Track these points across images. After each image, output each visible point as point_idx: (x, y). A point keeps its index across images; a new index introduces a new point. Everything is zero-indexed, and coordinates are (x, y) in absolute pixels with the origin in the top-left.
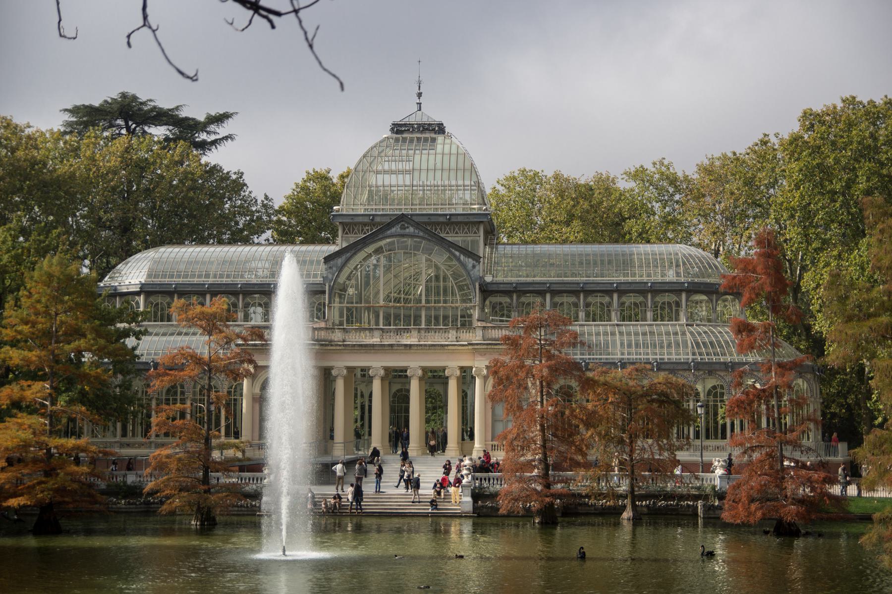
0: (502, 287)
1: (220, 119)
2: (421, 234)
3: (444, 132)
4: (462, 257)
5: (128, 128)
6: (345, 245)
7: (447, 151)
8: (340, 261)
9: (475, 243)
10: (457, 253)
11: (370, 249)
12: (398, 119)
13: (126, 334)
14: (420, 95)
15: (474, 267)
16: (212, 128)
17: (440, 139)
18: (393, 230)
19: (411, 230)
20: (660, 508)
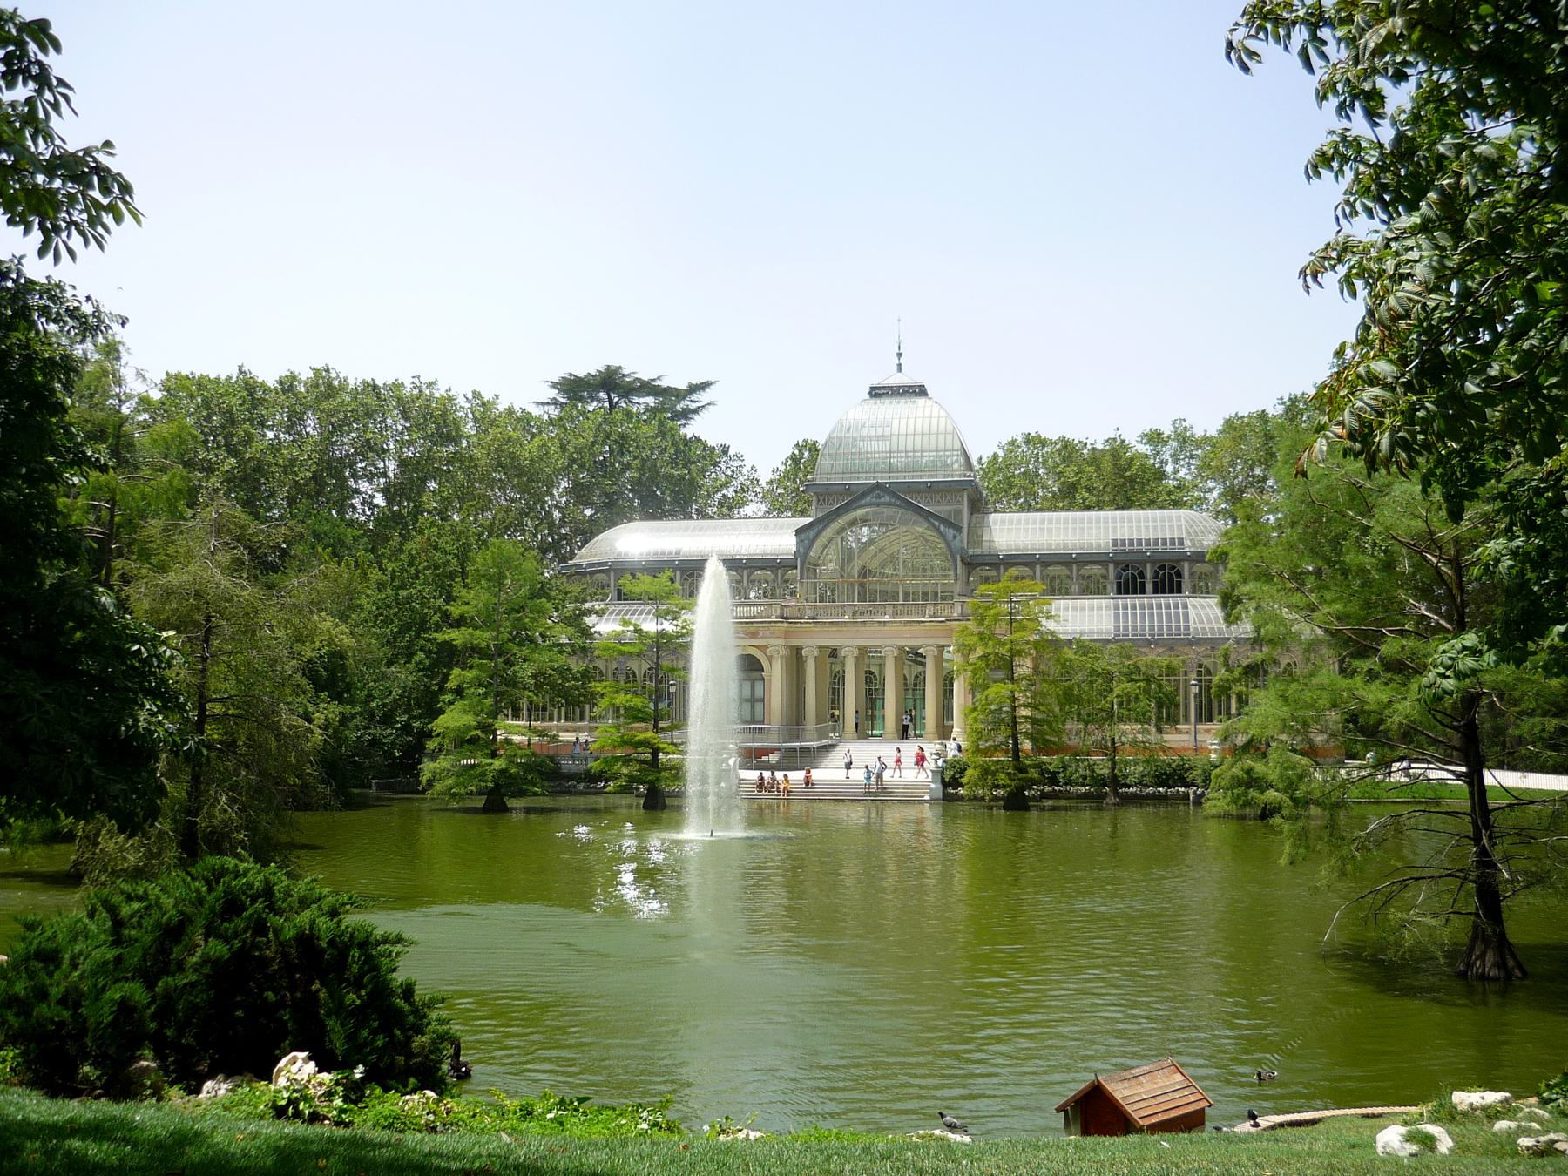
0: (987, 560)
1: (703, 386)
2: (898, 503)
3: (926, 395)
4: (942, 527)
5: (610, 401)
6: (820, 515)
7: (927, 414)
8: (811, 534)
9: (958, 513)
10: (937, 523)
11: (841, 521)
12: (875, 383)
13: (589, 612)
14: (900, 355)
15: (955, 537)
16: (695, 397)
17: (921, 401)
18: (868, 499)
19: (887, 499)
20: (1148, 794)
